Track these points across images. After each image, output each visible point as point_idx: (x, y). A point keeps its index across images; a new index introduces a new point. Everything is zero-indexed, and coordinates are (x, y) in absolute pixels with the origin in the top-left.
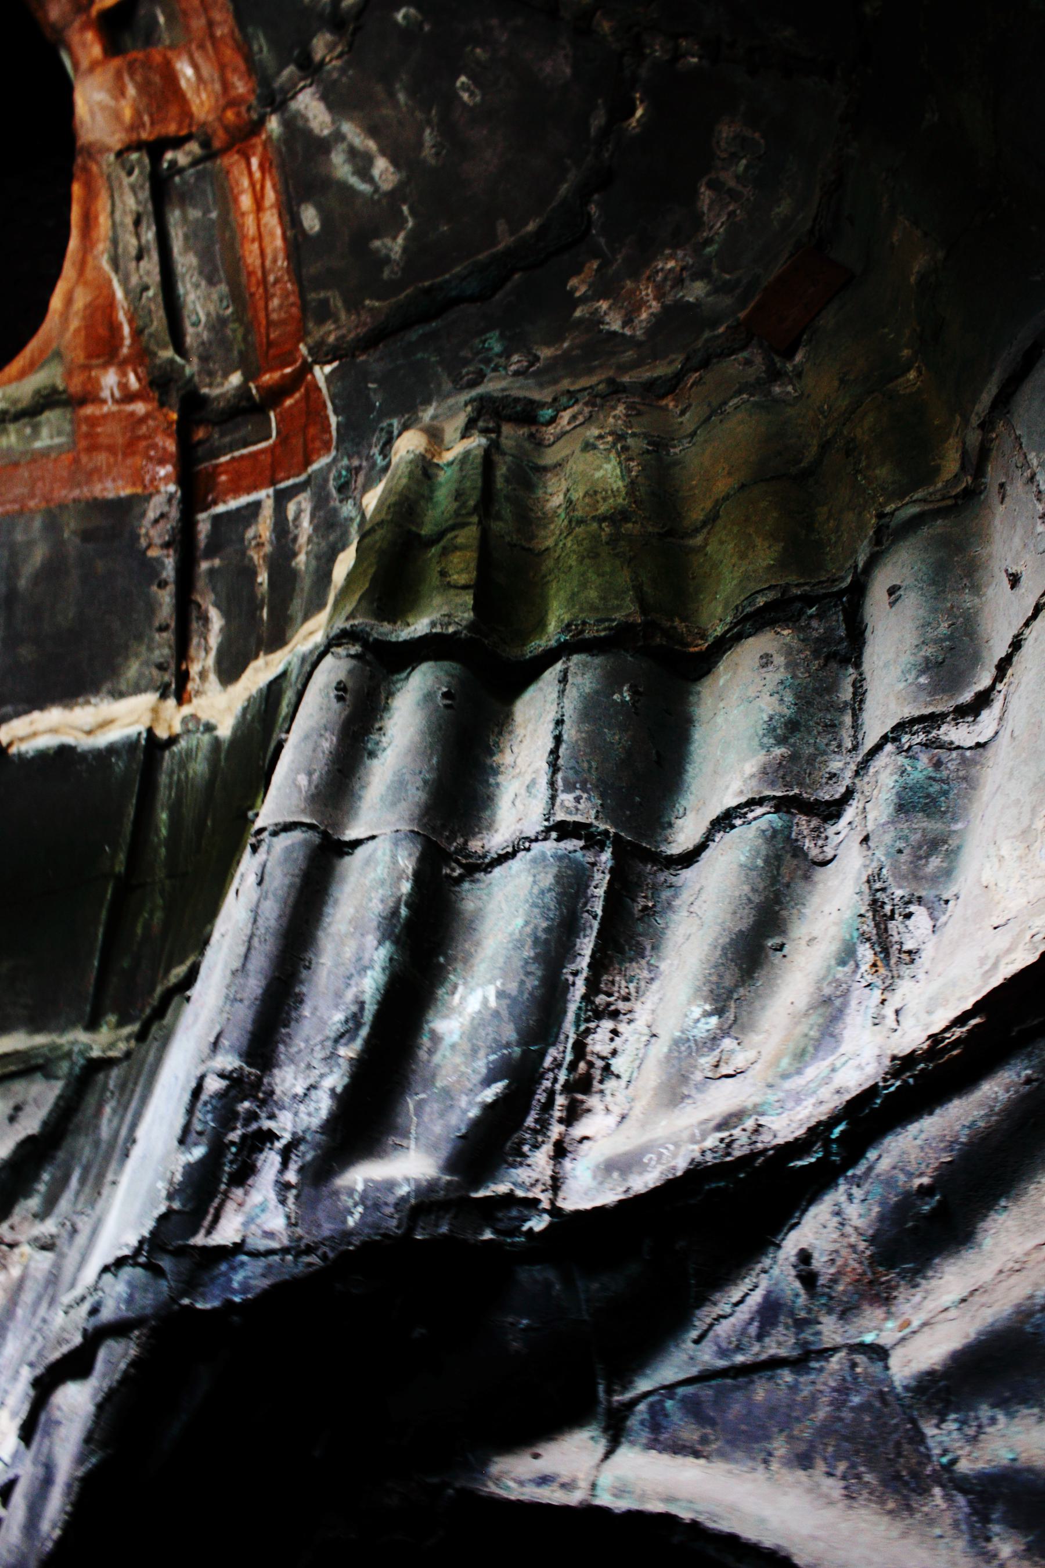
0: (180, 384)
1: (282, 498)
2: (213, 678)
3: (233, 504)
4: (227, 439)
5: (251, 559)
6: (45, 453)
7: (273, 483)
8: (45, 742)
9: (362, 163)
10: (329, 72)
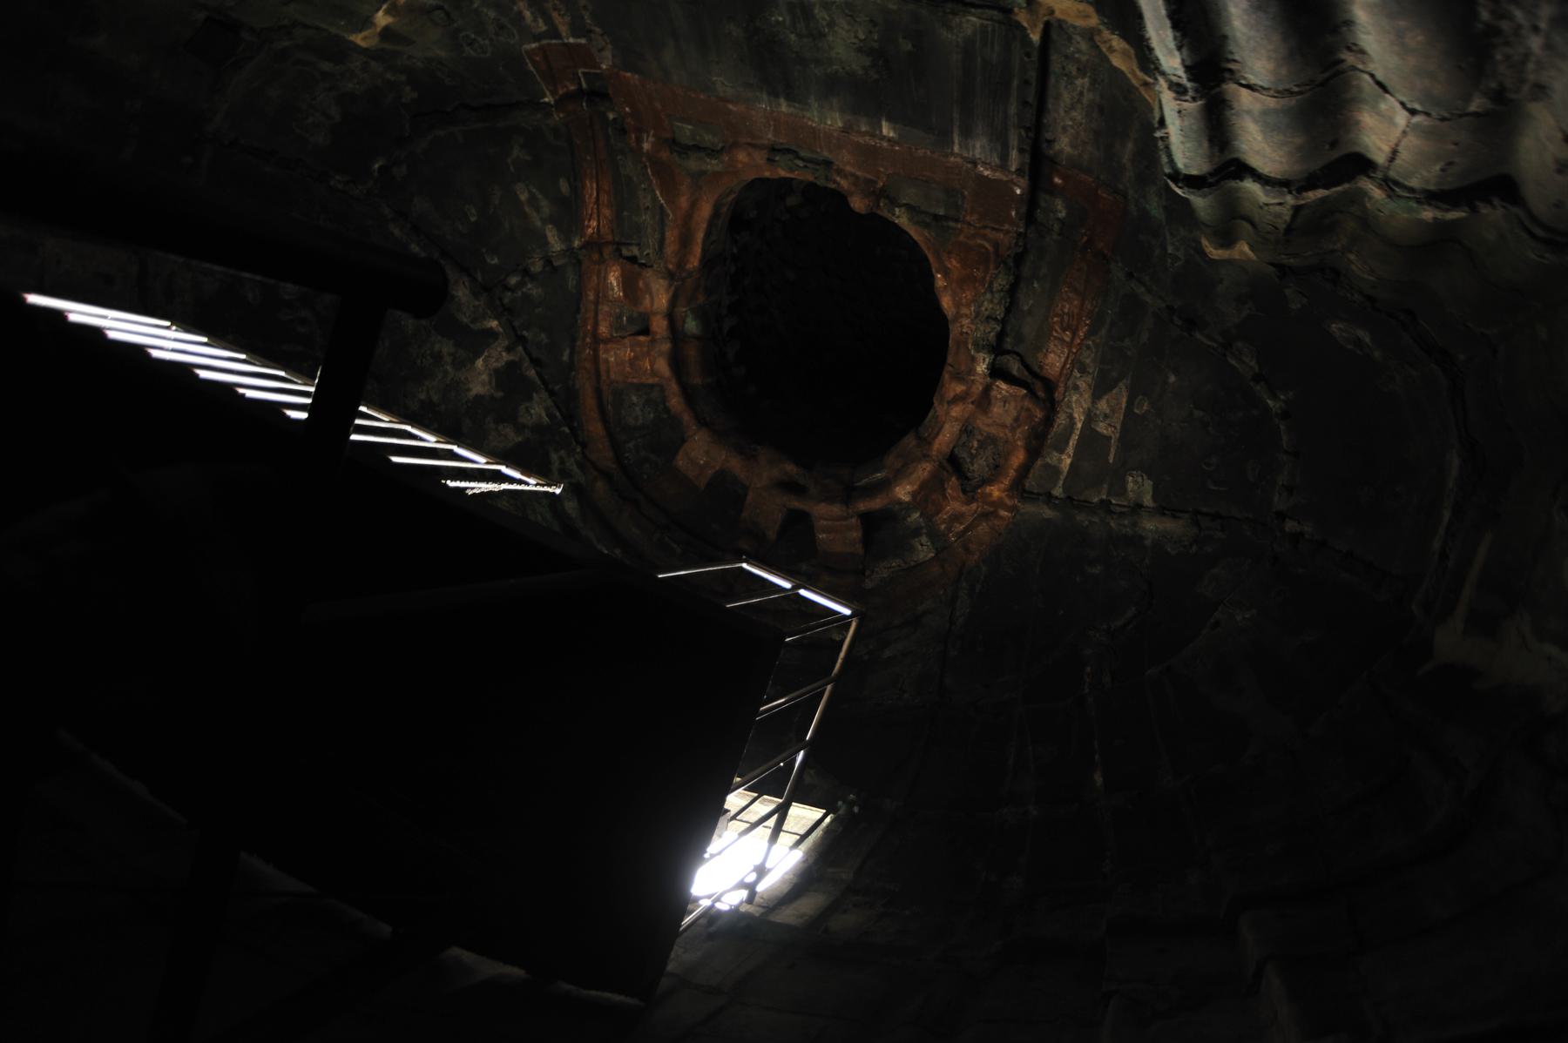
1: (554, 33)
7: (567, 45)
9: (532, 200)
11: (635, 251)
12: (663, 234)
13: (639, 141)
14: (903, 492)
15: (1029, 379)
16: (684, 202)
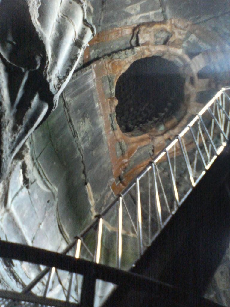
7: (113, 191)
11: (151, 151)
12: (144, 146)
13: (126, 163)
14: (180, 51)
16: (134, 145)
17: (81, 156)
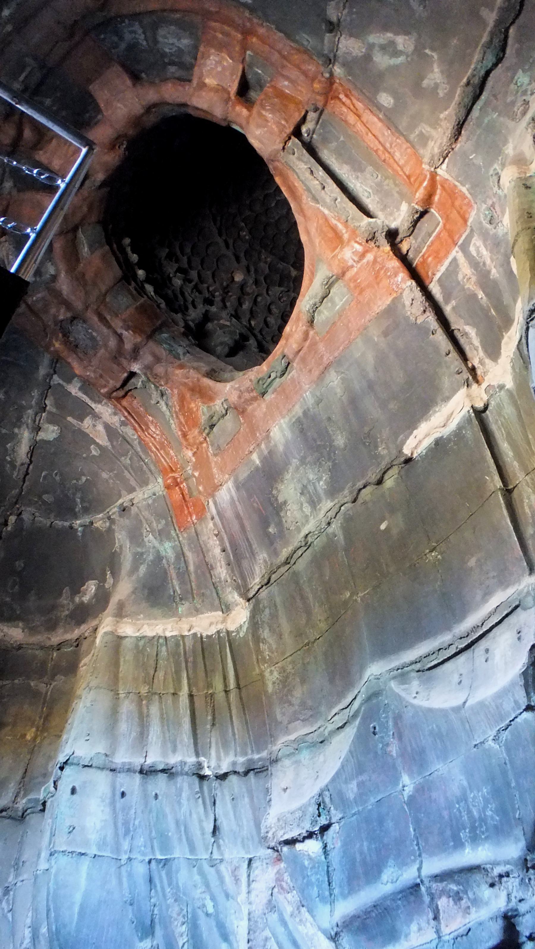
0: (380, 232)
1: (464, 249)
2: (487, 361)
3: (443, 269)
4: (419, 240)
5: (469, 289)
6: (343, 309)
8: (428, 442)
10: (345, 20)
15: (127, 388)
17: (342, 508)
